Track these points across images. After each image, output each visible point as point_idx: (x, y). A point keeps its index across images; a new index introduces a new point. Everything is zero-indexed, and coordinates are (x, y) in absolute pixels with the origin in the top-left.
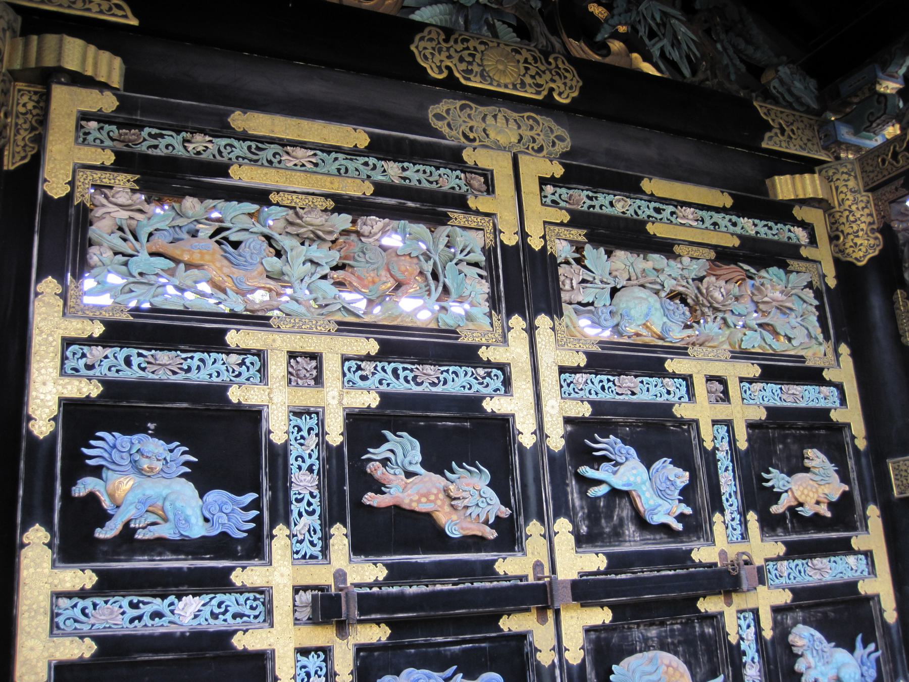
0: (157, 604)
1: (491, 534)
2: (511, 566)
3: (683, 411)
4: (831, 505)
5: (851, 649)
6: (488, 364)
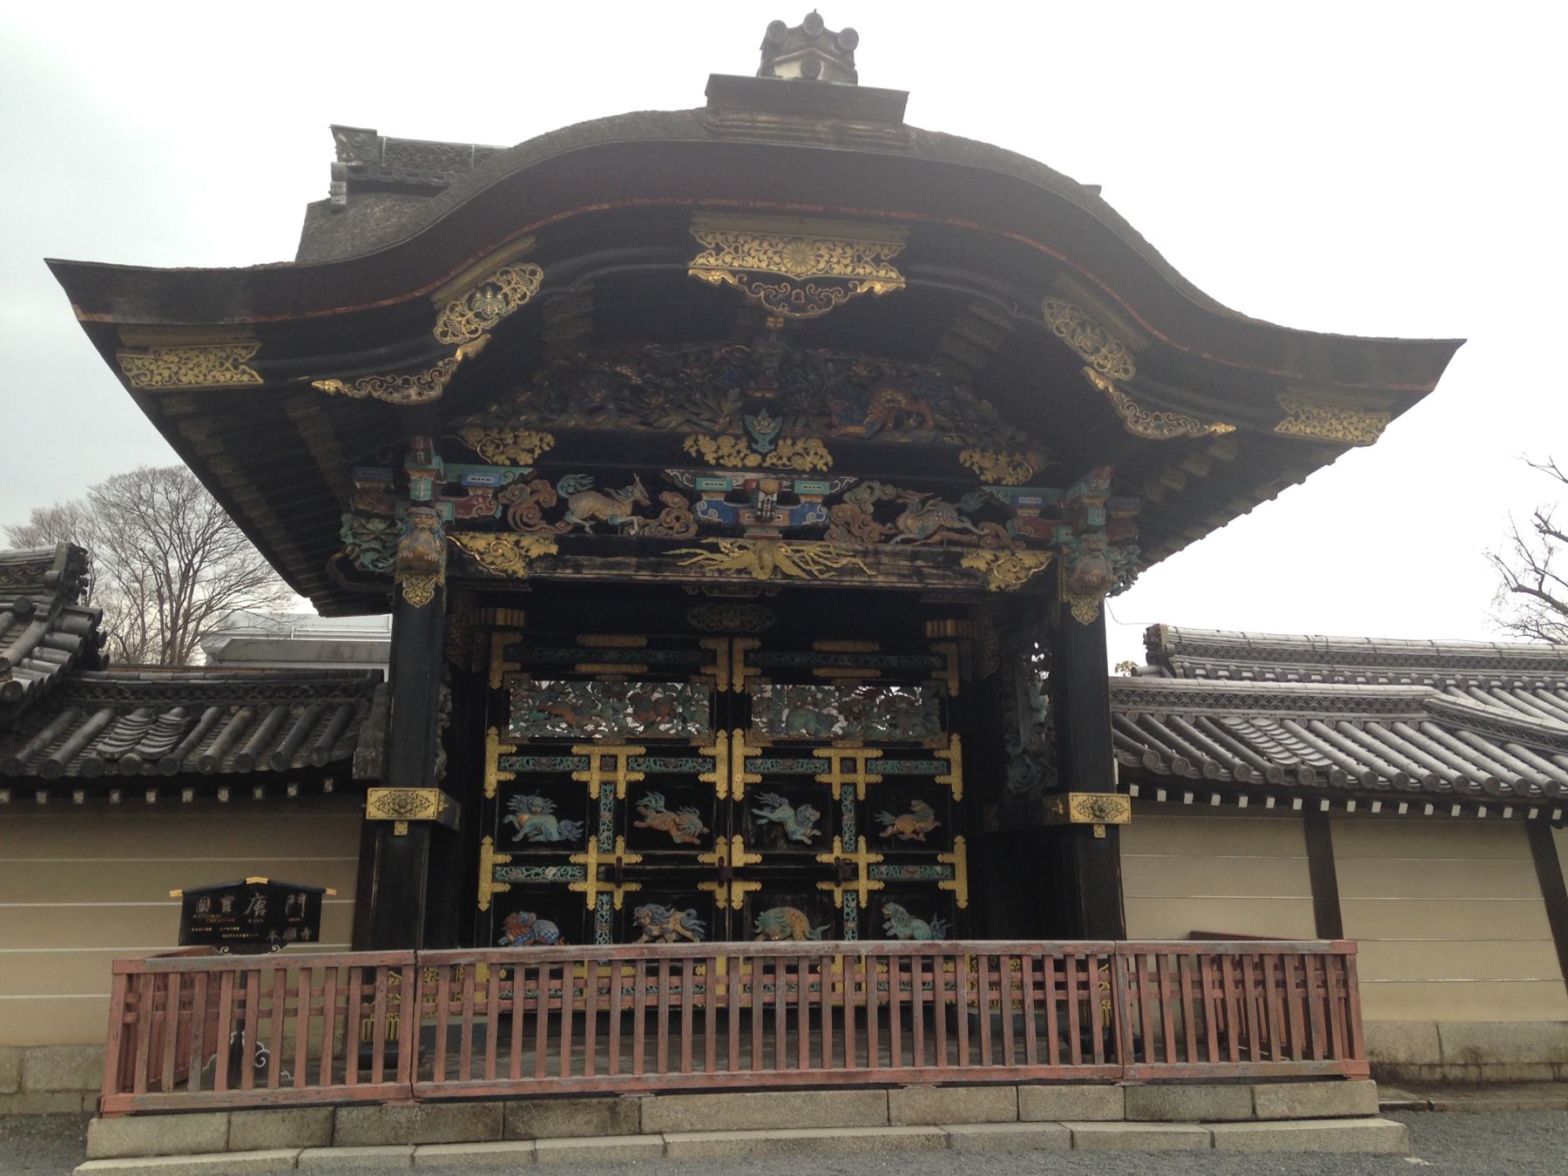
0: (537, 870)
1: (697, 842)
2: (706, 858)
3: (823, 778)
4: (926, 835)
5: (929, 922)
6: (704, 756)
